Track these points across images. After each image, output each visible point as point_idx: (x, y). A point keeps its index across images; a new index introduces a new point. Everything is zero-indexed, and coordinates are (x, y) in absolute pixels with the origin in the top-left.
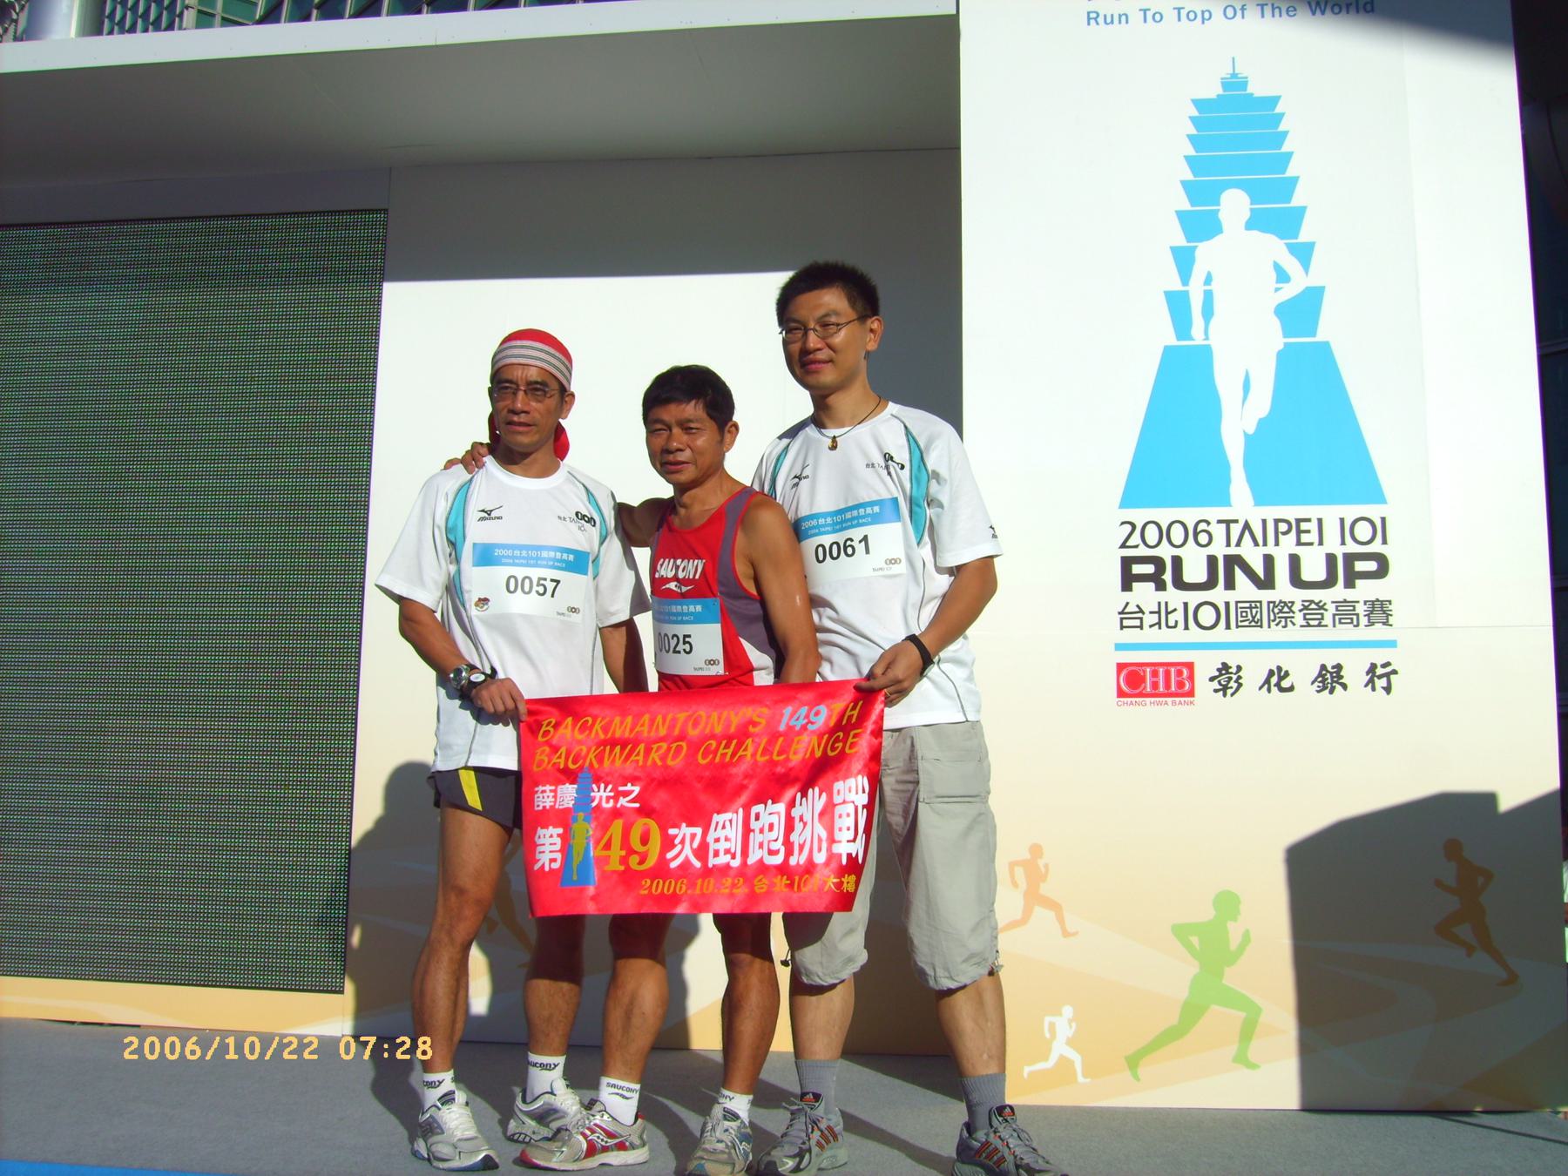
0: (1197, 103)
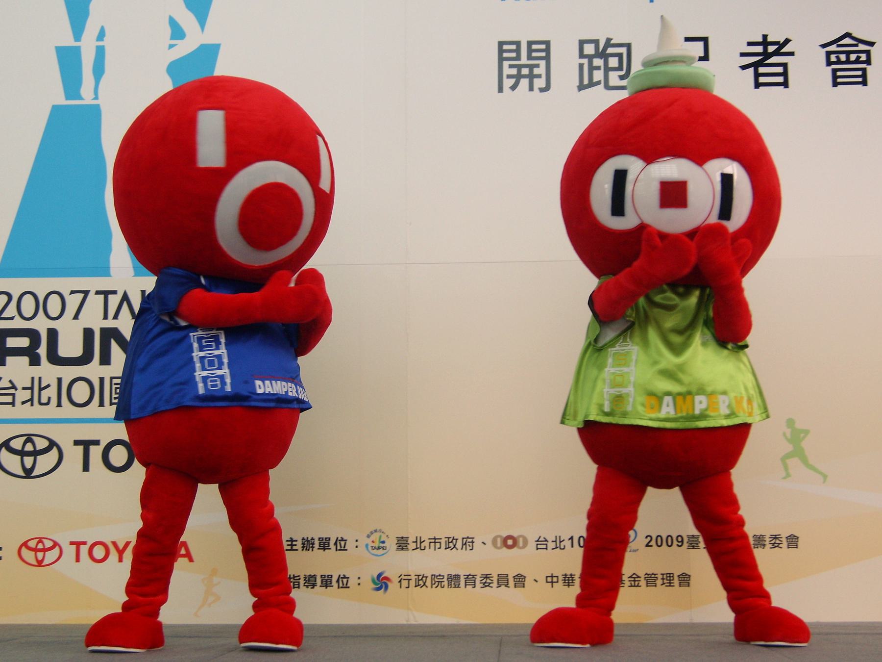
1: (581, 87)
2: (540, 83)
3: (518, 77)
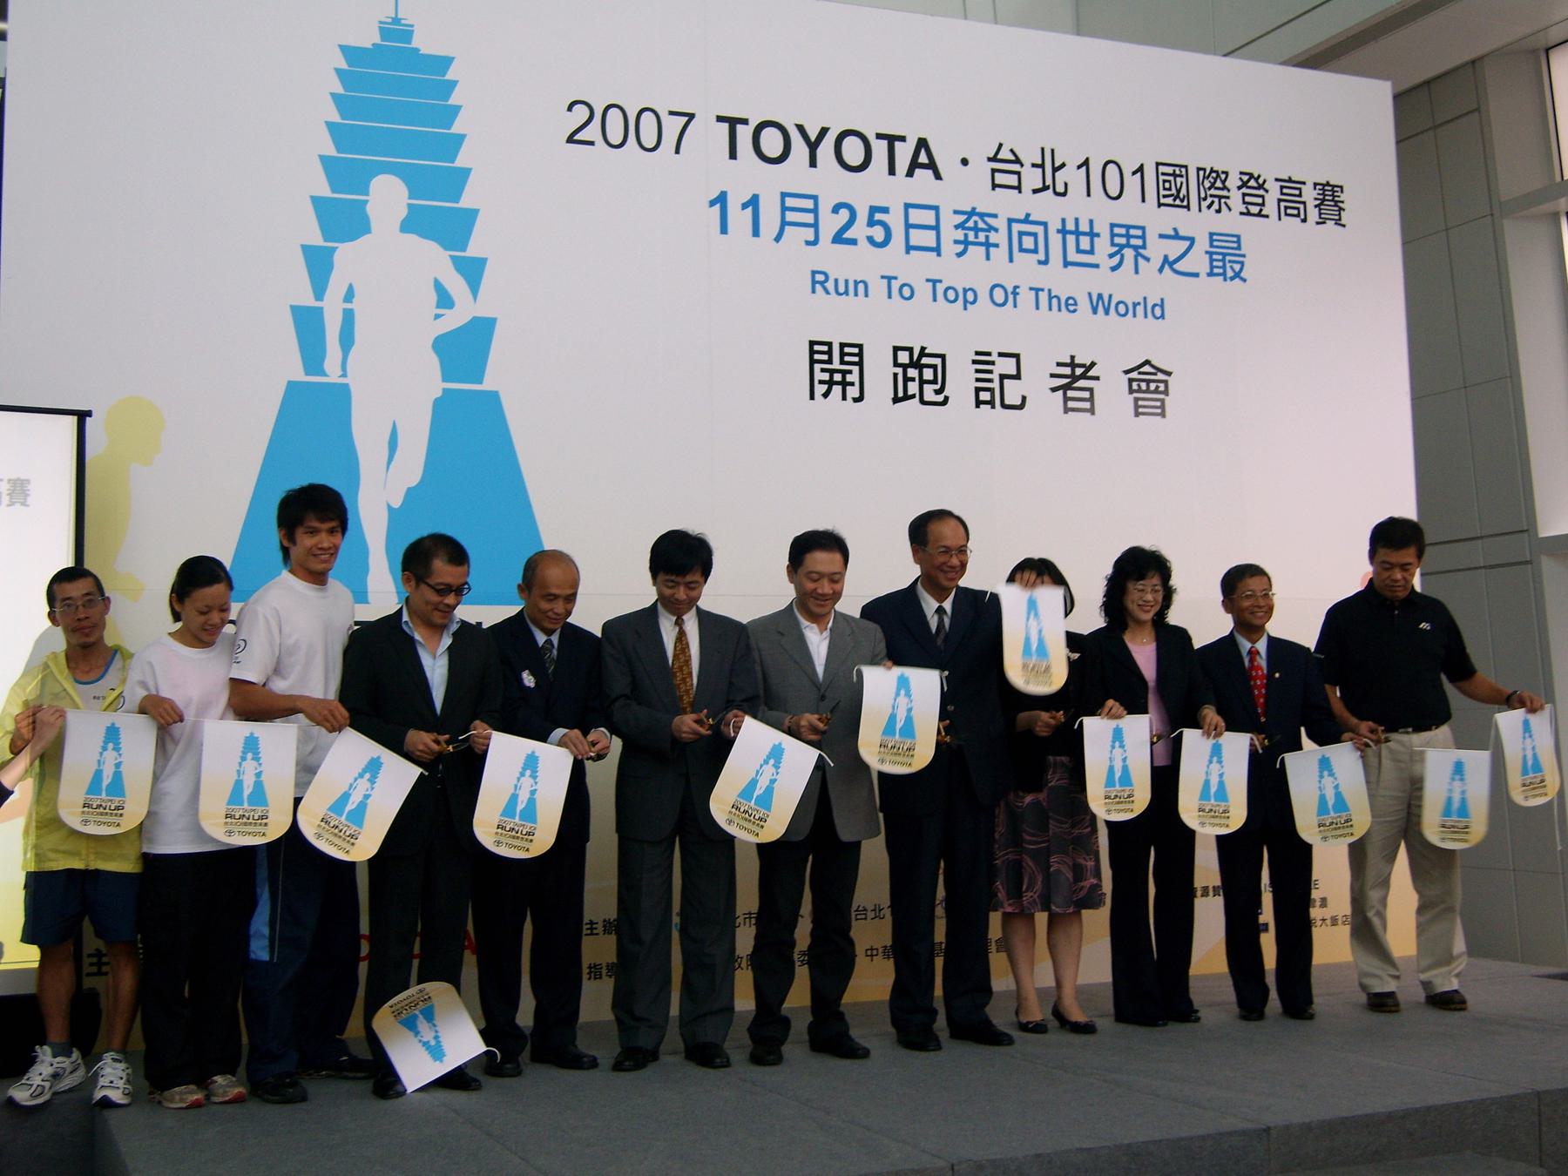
0: (344, 49)
1: (896, 400)
2: (853, 392)
3: (831, 383)
